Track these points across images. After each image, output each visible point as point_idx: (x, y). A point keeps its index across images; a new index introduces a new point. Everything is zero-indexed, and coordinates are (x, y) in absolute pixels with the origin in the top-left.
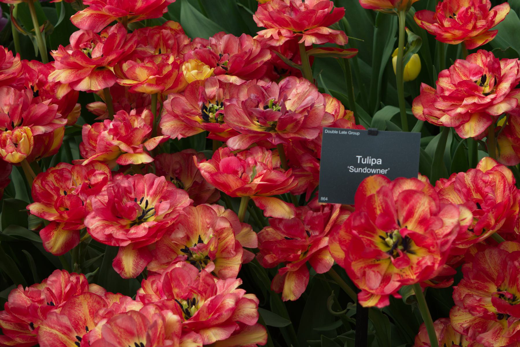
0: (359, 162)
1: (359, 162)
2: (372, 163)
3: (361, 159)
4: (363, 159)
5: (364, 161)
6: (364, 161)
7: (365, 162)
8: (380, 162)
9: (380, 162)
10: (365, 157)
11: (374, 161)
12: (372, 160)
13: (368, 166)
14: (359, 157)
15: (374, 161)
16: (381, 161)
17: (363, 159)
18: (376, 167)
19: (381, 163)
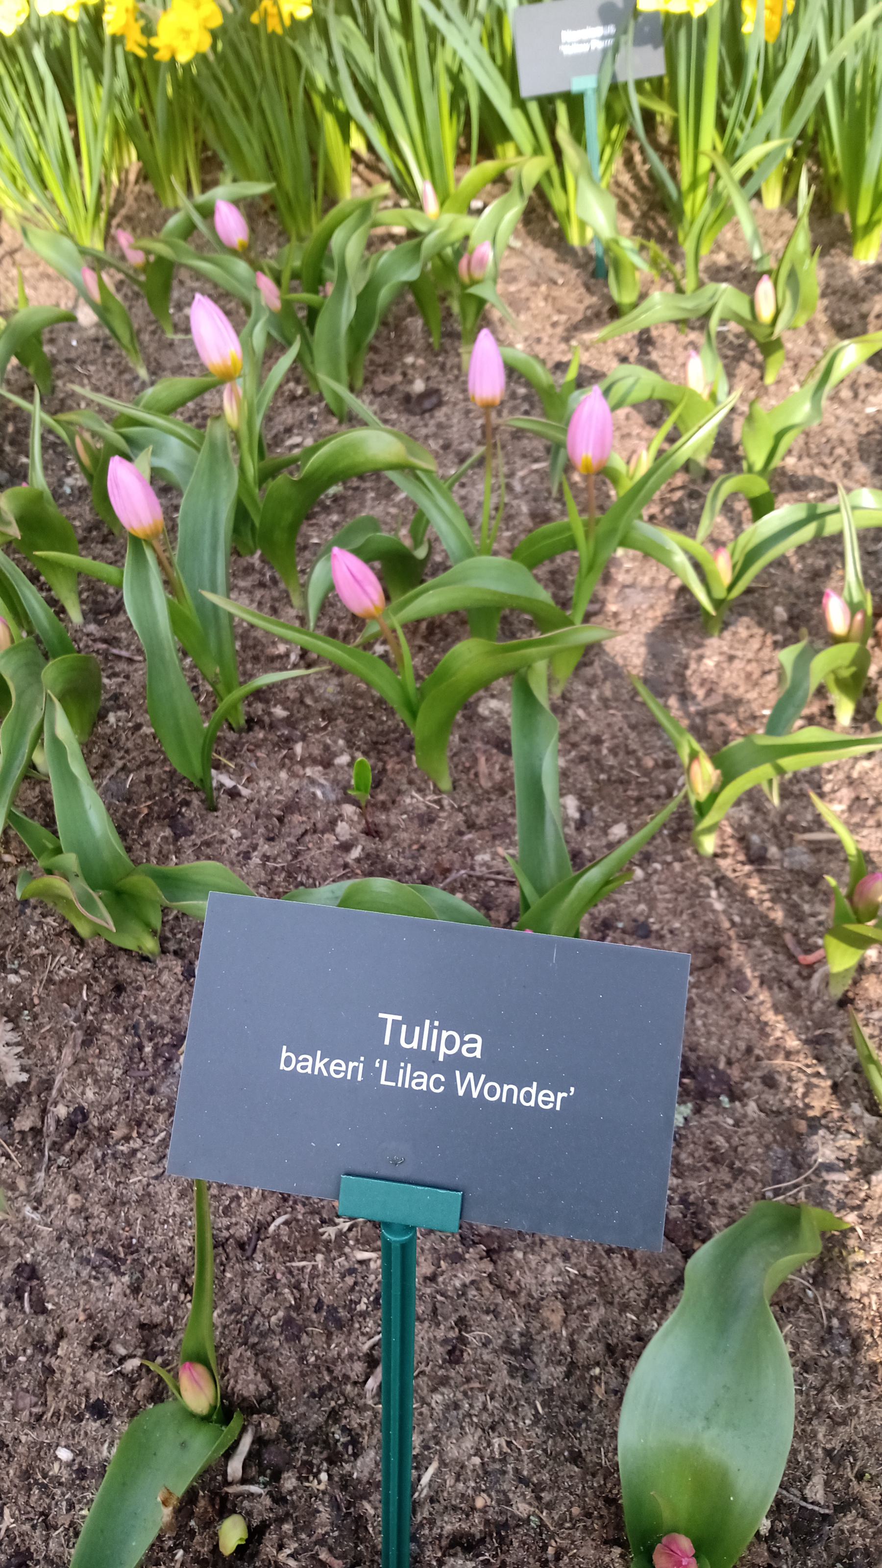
0: (387, 1042)
1: (387, 1042)
2: (443, 1049)
3: (396, 1025)
4: (404, 1027)
5: (409, 1040)
6: (409, 1040)
7: (414, 1045)
8: (474, 1046)
10: (413, 1021)
12: (445, 1034)
13: (425, 1061)
14: (390, 1018)
16: (479, 1045)
17: (404, 1027)
19: (478, 1054)
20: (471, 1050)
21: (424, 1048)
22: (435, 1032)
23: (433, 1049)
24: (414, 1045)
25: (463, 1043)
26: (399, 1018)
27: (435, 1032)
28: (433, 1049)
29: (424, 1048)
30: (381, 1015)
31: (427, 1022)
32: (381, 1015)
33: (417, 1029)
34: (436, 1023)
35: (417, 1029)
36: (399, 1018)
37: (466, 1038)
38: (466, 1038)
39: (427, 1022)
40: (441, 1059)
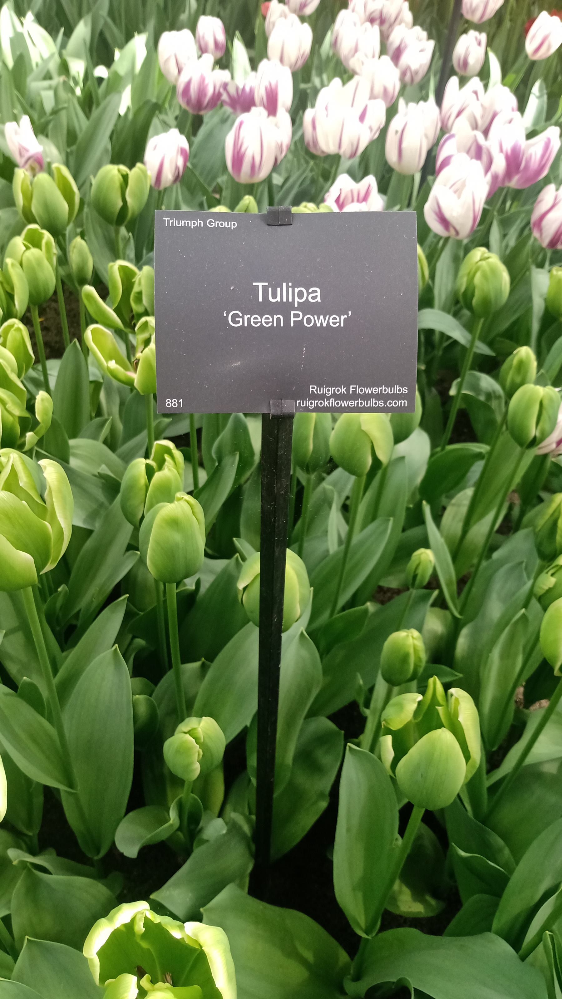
0: (260, 300)
1: (260, 300)
2: (297, 299)
3: (265, 289)
4: (270, 289)
5: (274, 296)
6: (274, 296)
7: (278, 299)
8: (315, 295)
9: (315, 295)
11: (300, 295)
13: (285, 308)
14: (260, 285)
15: (300, 295)
17: (270, 289)
18: (306, 308)
19: (319, 299)
20: (313, 298)
21: (285, 300)
22: (290, 289)
23: (290, 300)
24: (278, 299)
25: (308, 294)
26: (266, 284)
27: (290, 289)
28: (290, 300)
29: (285, 300)
30: (254, 284)
31: (284, 284)
32: (254, 284)
33: (279, 289)
34: (290, 284)
35: (279, 289)
36: (266, 284)
37: (310, 291)
38: (310, 291)
39: (284, 284)
40: (296, 305)
